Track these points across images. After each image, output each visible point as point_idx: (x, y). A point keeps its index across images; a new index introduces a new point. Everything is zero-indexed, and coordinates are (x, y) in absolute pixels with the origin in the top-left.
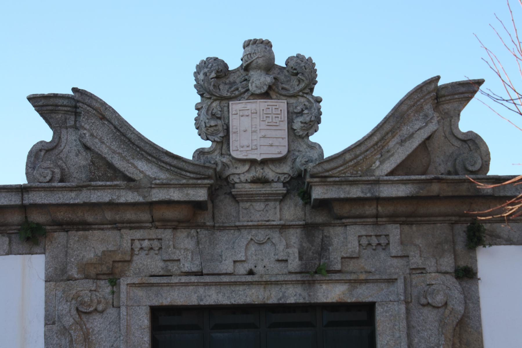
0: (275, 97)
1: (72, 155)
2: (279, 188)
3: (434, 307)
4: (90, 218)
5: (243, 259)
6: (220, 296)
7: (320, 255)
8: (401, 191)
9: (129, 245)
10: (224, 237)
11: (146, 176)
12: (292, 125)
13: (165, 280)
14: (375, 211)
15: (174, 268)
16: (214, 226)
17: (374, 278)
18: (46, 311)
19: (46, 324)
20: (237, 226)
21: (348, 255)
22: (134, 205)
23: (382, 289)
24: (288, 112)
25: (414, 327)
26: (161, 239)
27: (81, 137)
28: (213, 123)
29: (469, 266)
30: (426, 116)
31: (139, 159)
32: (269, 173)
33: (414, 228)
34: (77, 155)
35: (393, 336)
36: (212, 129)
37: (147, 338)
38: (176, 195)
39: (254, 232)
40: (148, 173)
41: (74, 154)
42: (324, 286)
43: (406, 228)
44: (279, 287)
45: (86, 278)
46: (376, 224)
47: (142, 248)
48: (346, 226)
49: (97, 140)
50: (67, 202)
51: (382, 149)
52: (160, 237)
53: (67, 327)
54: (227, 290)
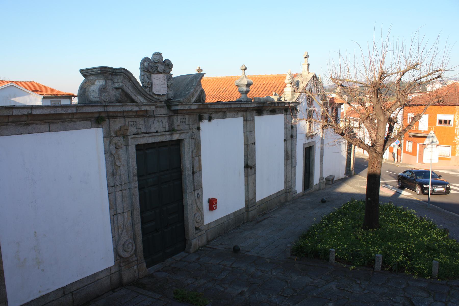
1: (111, 90)
4: (119, 115)
7: (171, 124)
10: (151, 120)
11: (141, 101)
15: (139, 131)
18: (105, 148)
19: (105, 154)
31: (139, 95)
33: (190, 116)
34: (112, 90)
40: (141, 100)
42: (174, 135)
45: (117, 136)
49: (127, 88)
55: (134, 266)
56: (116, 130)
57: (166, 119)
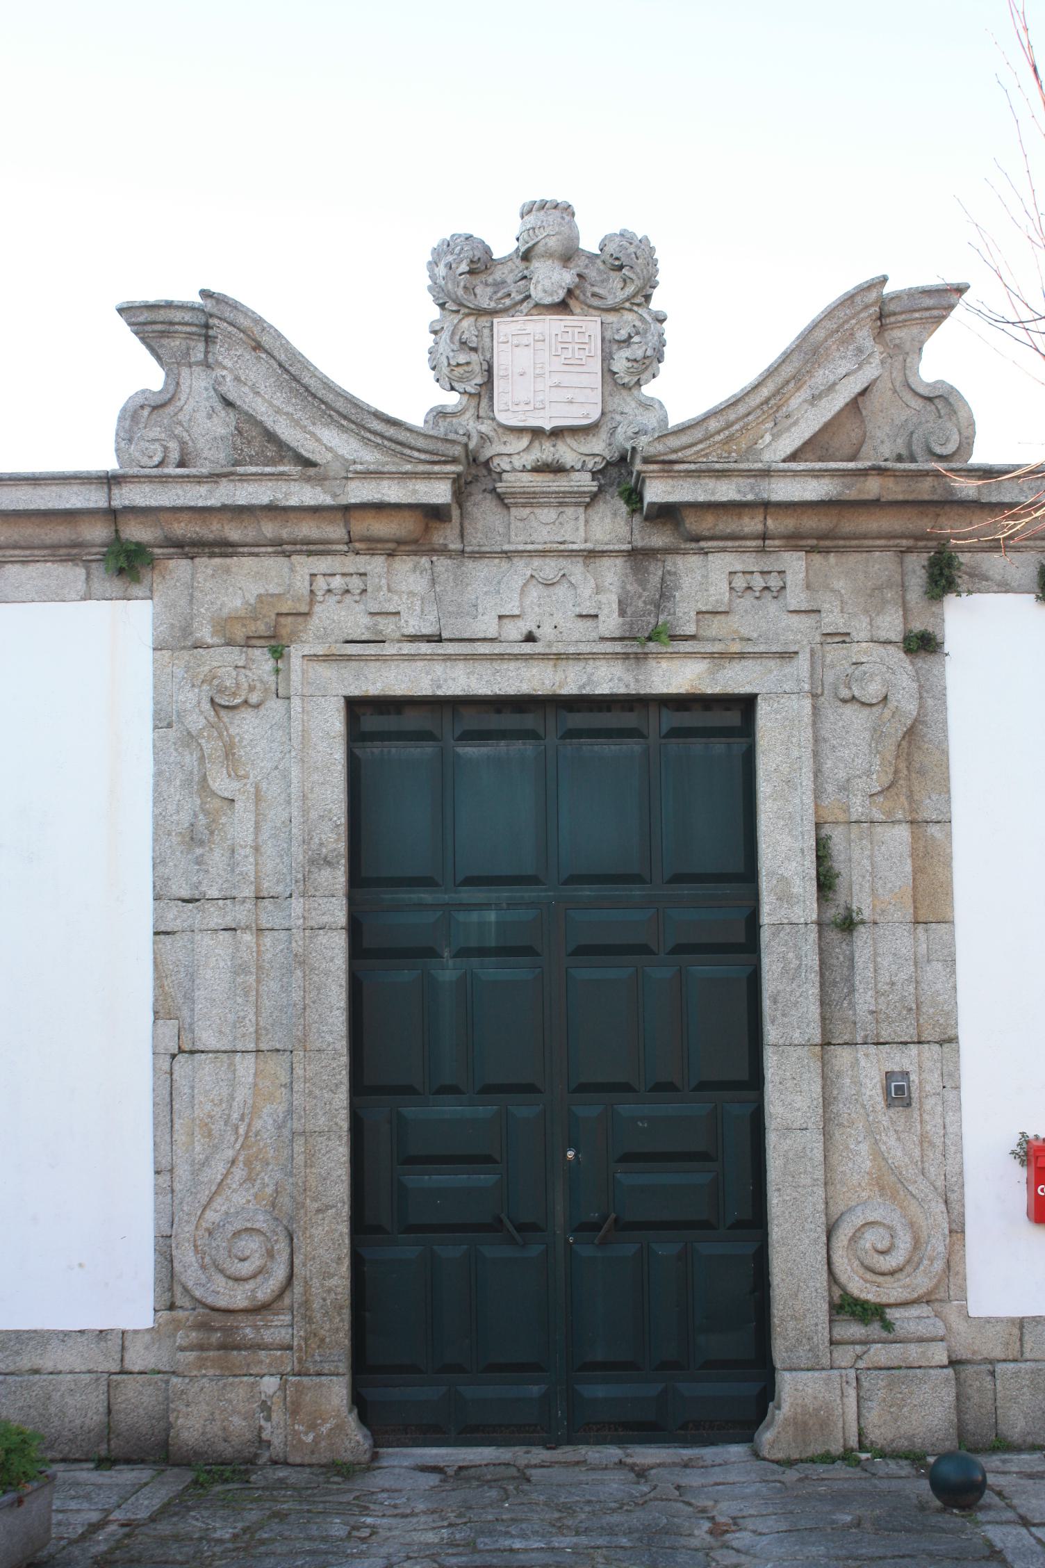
0: (577, 310)
1: (201, 416)
2: (584, 482)
3: (863, 704)
5: (517, 612)
6: (473, 679)
7: (658, 606)
8: (812, 490)
9: (307, 584)
10: (480, 571)
11: (337, 456)
12: (609, 364)
13: (371, 649)
14: (760, 527)
15: (388, 627)
16: (463, 551)
17: (756, 650)
18: (156, 703)
19: (156, 727)
20: (506, 552)
21: (709, 608)
22: (316, 510)
23: (771, 671)
24: (603, 340)
25: (825, 740)
26: (365, 574)
27: (217, 383)
28: (462, 358)
29: (930, 630)
30: (860, 350)
31: (326, 425)
32: (566, 452)
33: (832, 558)
35: (788, 756)
36: (461, 370)
37: (339, 755)
38: (392, 492)
39: (537, 562)
40: (341, 451)
41: (204, 414)
42: (664, 664)
43: (817, 558)
44: (582, 664)
45: (228, 644)
46: (762, 550)
47: (329, 591)
48: (707, 553)
49: (246, 389)
50: (192, 504)
51: (777, 411)
52: (362, 571)
53: (194, 733)
54: (485, 669)
55: (262, 1376)
56: (226, 611)
57: (612, 572)
